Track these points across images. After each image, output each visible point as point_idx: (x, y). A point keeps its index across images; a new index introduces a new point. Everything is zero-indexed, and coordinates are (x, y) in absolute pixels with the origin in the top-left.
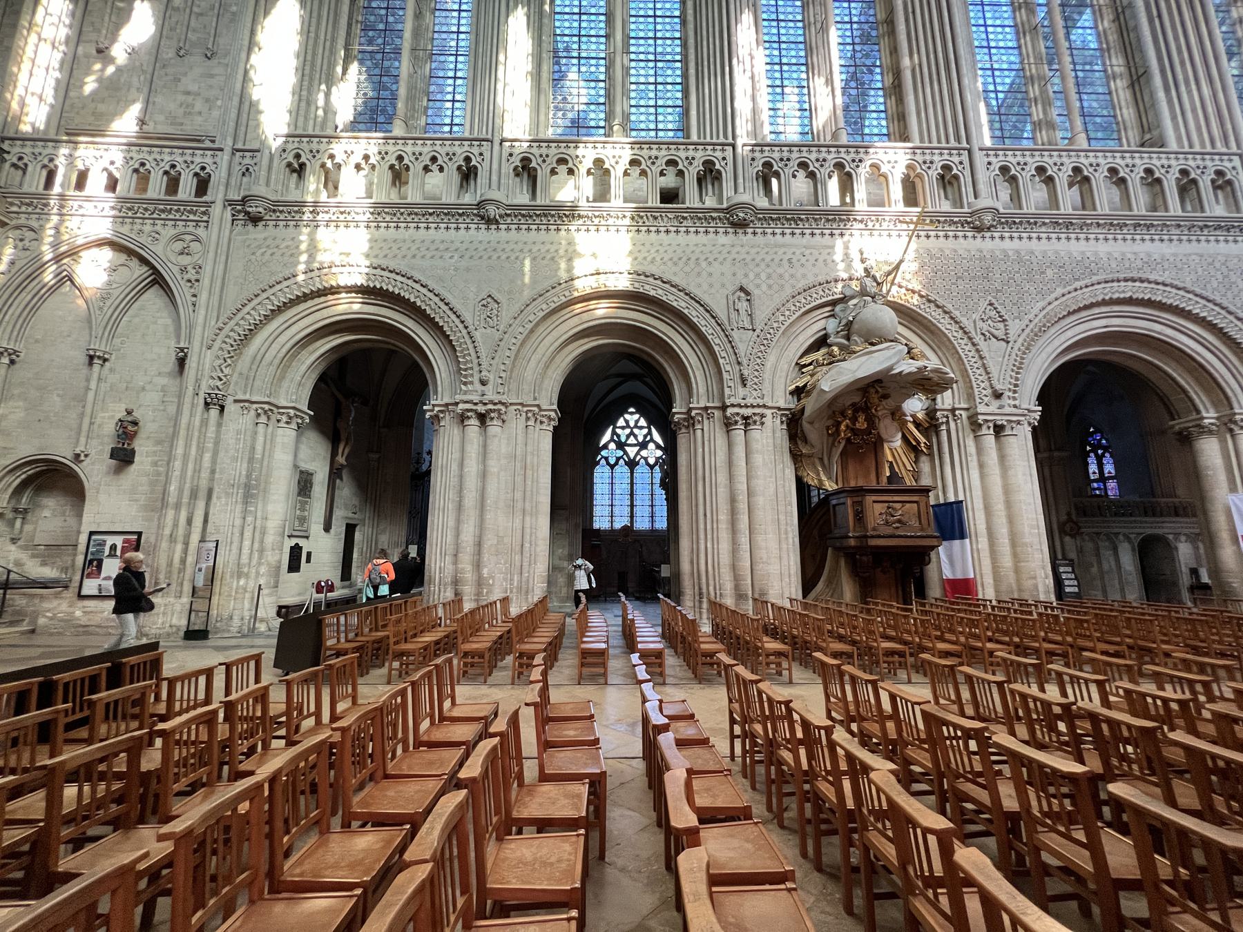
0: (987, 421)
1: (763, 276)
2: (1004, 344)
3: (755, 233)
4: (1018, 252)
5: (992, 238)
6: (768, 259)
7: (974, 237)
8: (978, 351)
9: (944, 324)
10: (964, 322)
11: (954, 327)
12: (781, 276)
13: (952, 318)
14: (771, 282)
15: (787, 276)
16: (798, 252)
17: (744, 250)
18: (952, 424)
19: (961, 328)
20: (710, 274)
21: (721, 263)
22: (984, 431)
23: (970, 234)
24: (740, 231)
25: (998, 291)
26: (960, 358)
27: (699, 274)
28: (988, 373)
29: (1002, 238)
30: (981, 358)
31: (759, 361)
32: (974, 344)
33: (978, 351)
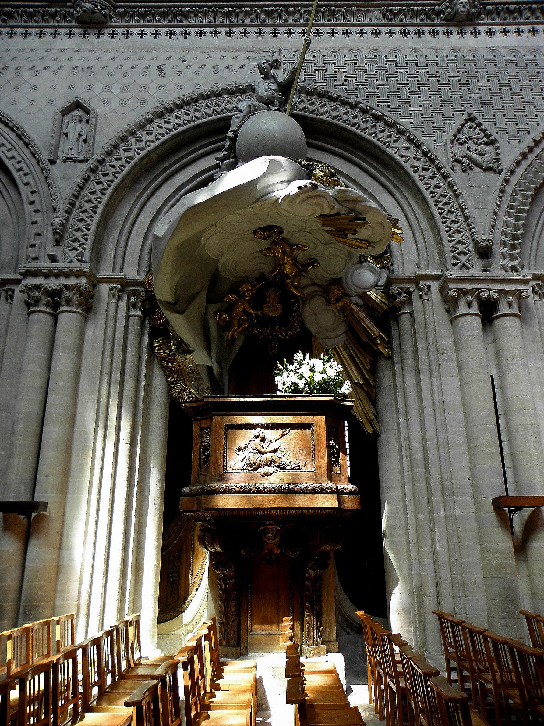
0: (464, 293)
1: (116, 89)
2: (496, 175)
3: (113, 35)
4: (514, 50)
5: (476, 33)
6: (127, 65)
7: (448, 33)
8: (451, 186)
9: (397, 151)
10: (429, 144)
11: (412, 153)
12: (143, 88)
13: (410, 140)
14: (126, 96)
15: (153, 88)
16: (175, 56)
17: (93, 56)
18: (417, 303)
19: (425, 154)
20: (35, 88)
21: (55, 73)
22: (463, 309)
23: (441, 29)
24: (92, 32)
25: (483, 102)
26: (424, 200)
27: (17, 88)
28: (467, 218)
29: (490, 33)
30: (457, 196)
31: (88, 206)
32: (445, 177)
33: (451, 186)
